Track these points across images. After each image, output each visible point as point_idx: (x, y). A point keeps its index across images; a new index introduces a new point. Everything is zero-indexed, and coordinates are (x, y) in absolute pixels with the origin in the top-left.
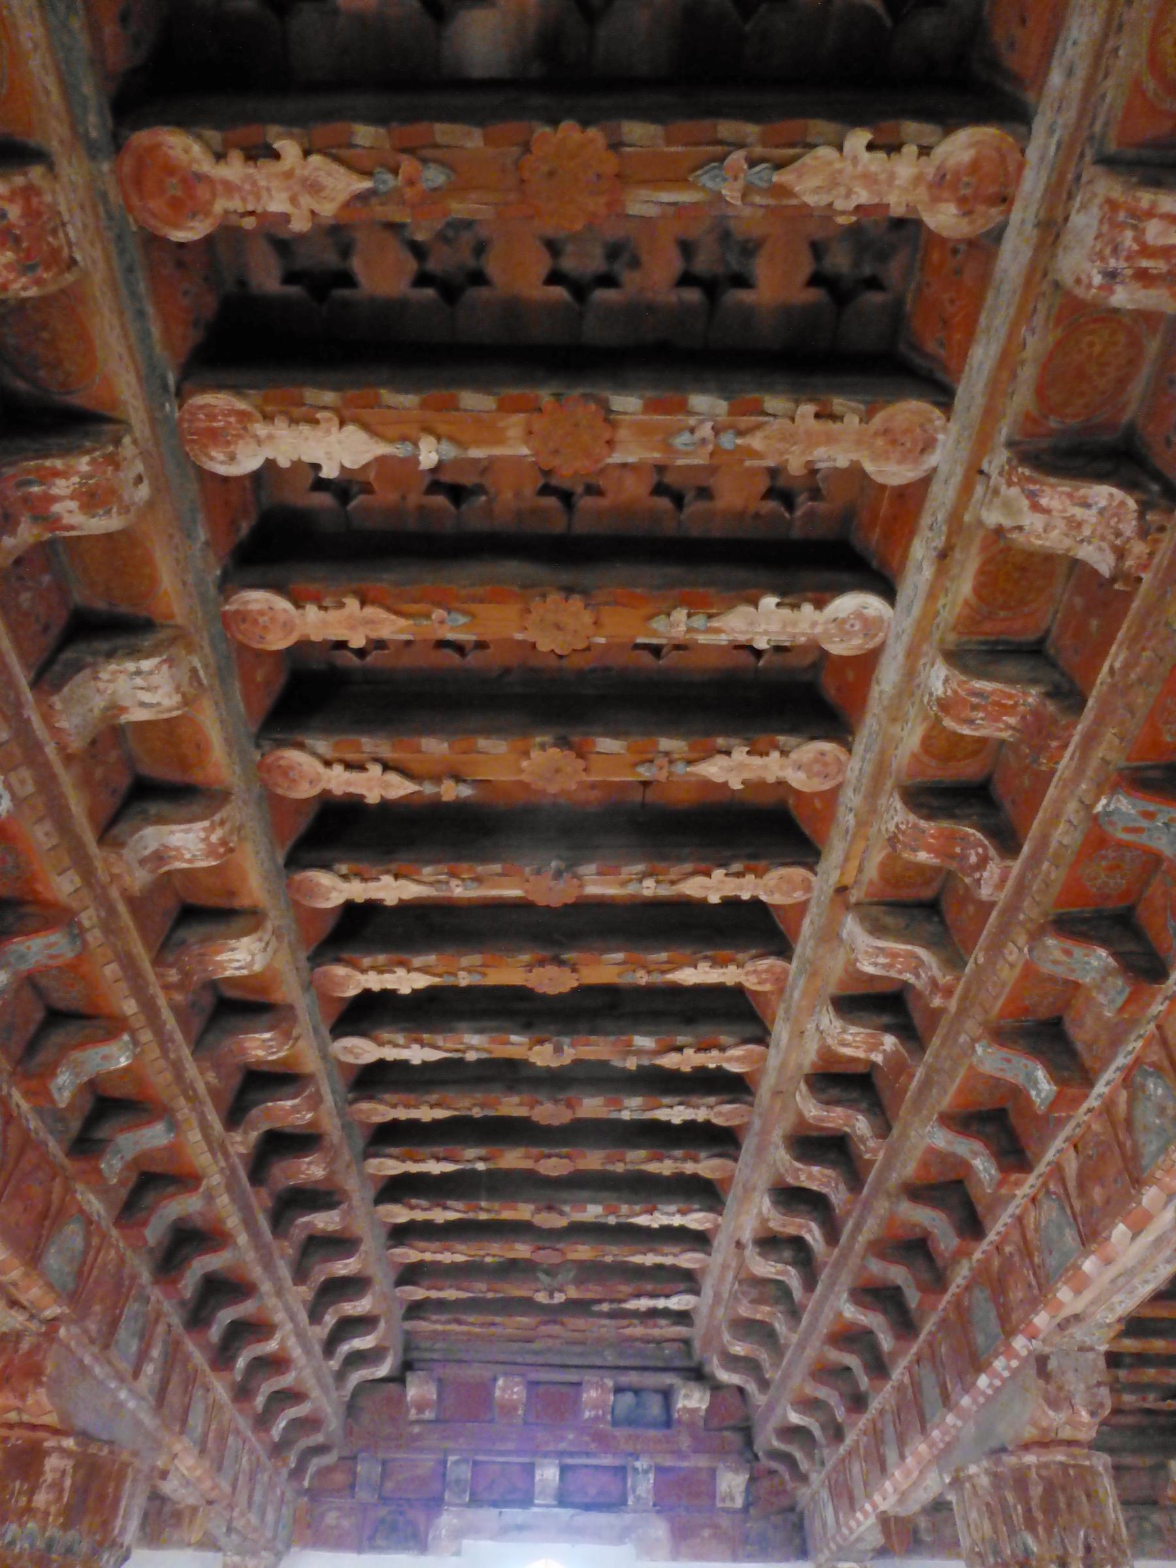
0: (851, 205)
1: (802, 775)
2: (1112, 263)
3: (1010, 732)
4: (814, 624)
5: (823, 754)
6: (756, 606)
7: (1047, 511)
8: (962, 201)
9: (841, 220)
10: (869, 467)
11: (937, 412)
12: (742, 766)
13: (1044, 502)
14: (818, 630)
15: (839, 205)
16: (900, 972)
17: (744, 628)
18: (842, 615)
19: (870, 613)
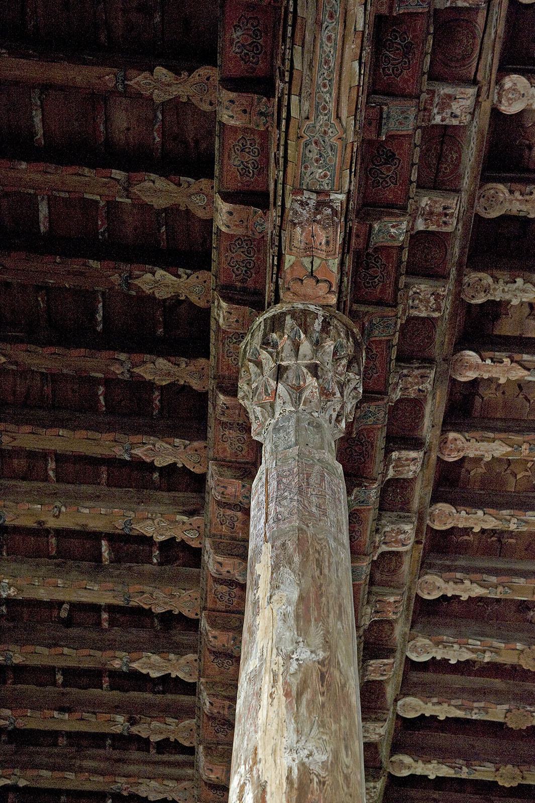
0: (433, 765)
1: (438, 584)
2: (375, 790)
3: (370, 664)
4: (436, 652)
5: (429, 594)
6: (458, 660)
7: (376, 734)
8: (402, 763)
9: (436, 762)
10: (421, 703)
11: (401, 714)
12: (465, 591)
13: (377, 736)
14: (434, 650)
15: (436, 765)
16: (393, 530)
17: (463, 653)
18: (425, 654)
19: (415, 654)
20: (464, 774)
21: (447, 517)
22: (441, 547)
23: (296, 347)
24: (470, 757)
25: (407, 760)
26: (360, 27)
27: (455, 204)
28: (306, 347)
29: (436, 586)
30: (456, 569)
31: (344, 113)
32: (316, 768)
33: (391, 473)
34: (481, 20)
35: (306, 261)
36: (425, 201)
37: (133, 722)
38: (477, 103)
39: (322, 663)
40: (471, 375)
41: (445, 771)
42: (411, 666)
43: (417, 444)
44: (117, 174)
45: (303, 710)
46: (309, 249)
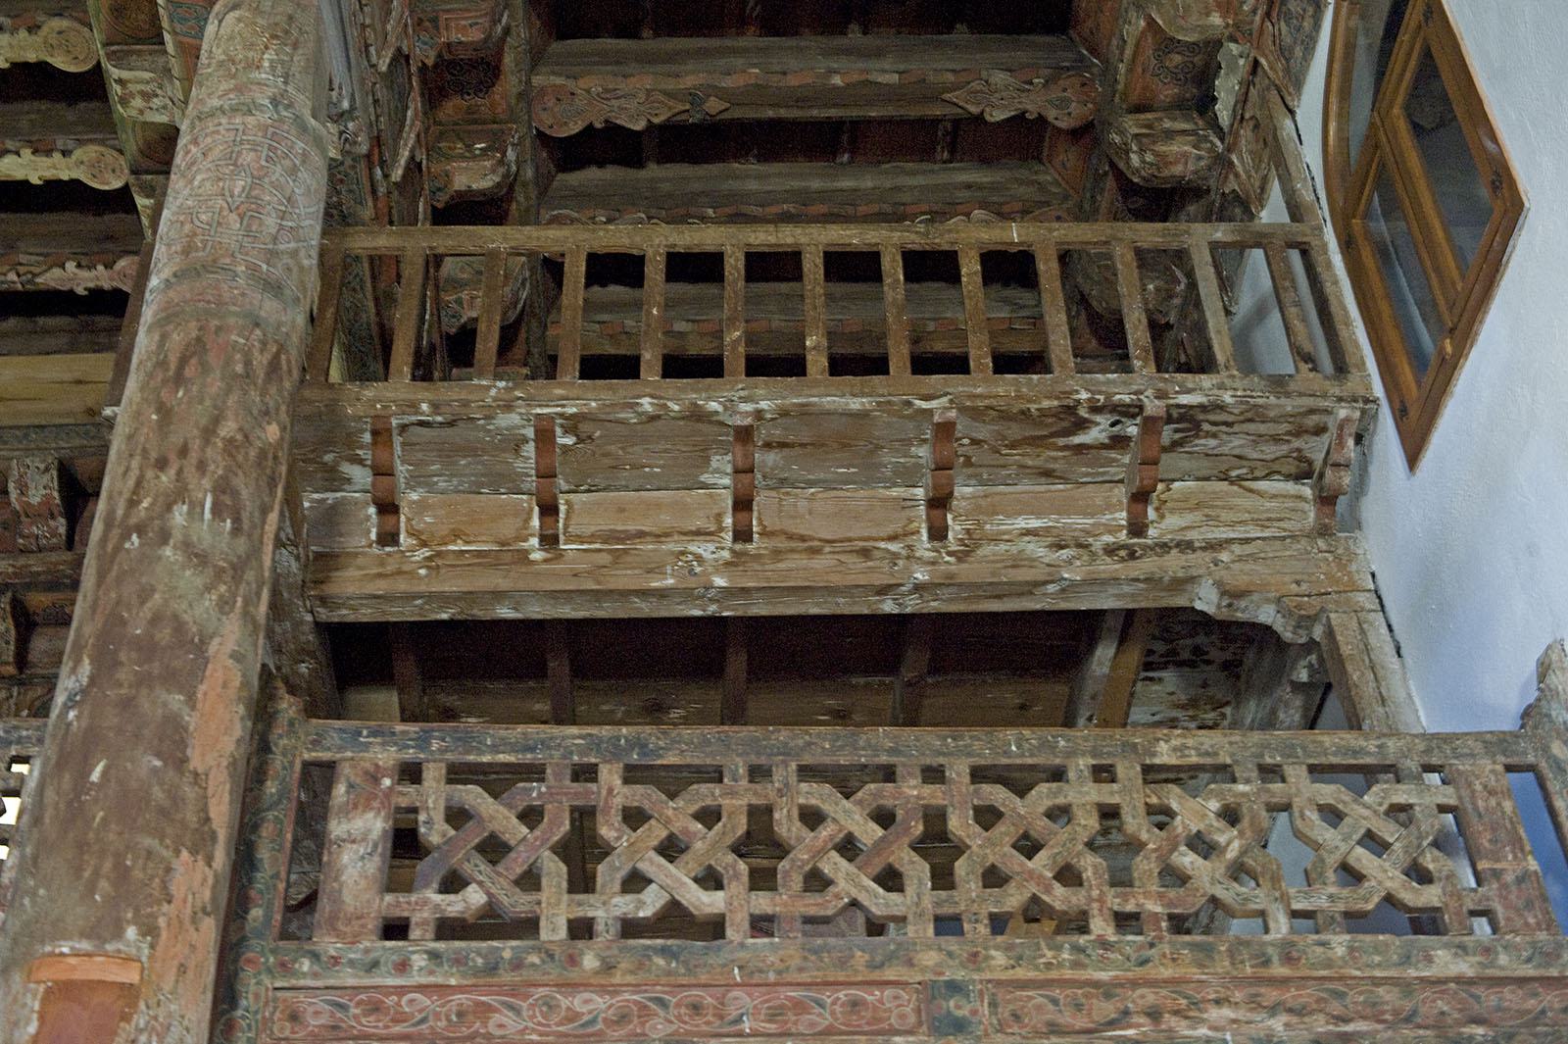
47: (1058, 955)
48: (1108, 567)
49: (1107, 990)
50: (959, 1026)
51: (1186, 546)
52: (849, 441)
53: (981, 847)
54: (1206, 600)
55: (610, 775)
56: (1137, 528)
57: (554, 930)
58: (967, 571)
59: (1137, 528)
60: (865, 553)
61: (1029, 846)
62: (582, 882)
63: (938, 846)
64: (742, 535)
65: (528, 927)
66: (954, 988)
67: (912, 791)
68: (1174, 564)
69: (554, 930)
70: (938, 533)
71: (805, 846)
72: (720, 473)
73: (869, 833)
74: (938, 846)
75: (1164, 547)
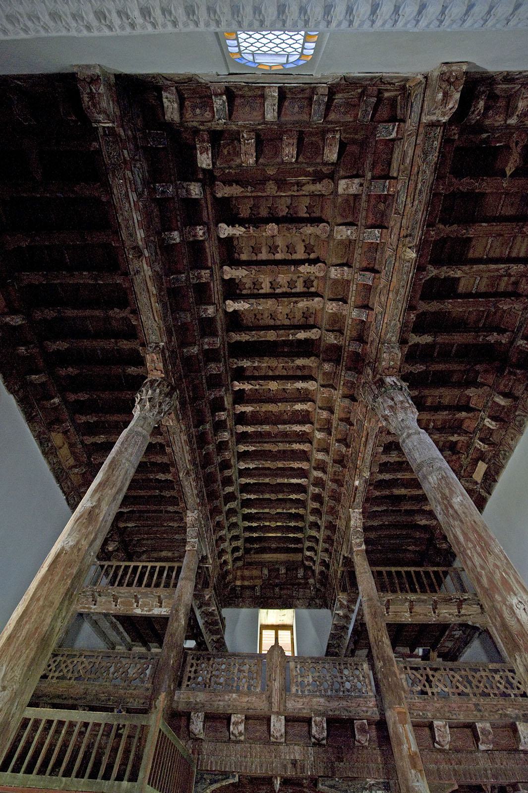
20: (261, 497)
21: (241, 429)
22: (243, 438)
23: (148, 391)
24: (263, 492)
25: (245, 495)
26: (155, 292)
27: (218, 341)
28: (150, 392)
29: (242, 448)
30: (248, 442)
31: (157, 319)
32: (67, 548)
33: (217, 419)
34: (212, 285)
35: (153, 365)
36: (206, 340)
37: (161, 492)
38: (217, 310)
39: (92, 507)
40: (237, 388)
41: (256, 497)
42: (240, 470)
43: (224, 410)
44: (113, 340)
45: (75, 526)
46: (153, 361)
47: (488, 699)
48: (457, 618)
49: (496, 705)
50: (480, 711)
51: (466, 615)
52: (424, 601)
53: (475, 682)
54: (470, 623)
55: (428, 669)
56: (459, 612)
57: (430, 694)
58: (441, 619)
59: (459, 612)
60: (426, 615)
61: (480, 682)
62: (431, 687)
63: (470, 683)
64: (411, 612)
65: (426, 693)
66: (478, 704)
67: (463, 672)
68: (464, 618)
69: (430, 694)
70: (435, 613)
71: (454, 680)
72: (407, 604)
73: (461, 679)
74: (470, 683)
75: (463, 615)
